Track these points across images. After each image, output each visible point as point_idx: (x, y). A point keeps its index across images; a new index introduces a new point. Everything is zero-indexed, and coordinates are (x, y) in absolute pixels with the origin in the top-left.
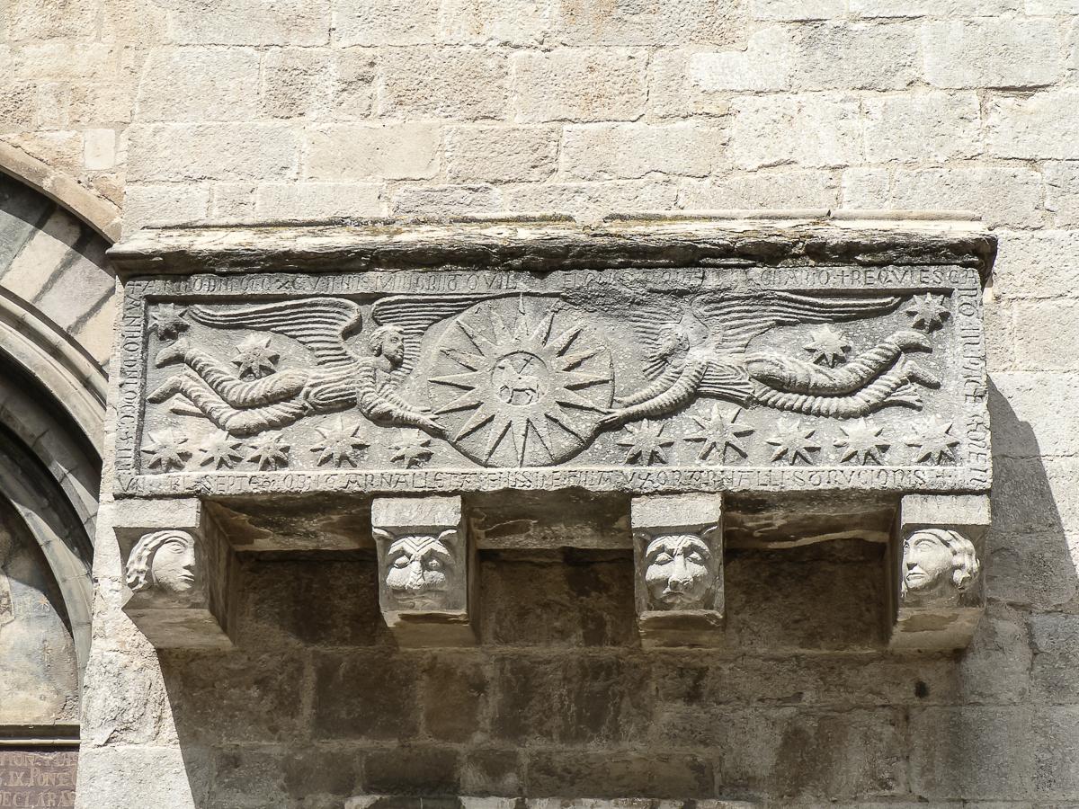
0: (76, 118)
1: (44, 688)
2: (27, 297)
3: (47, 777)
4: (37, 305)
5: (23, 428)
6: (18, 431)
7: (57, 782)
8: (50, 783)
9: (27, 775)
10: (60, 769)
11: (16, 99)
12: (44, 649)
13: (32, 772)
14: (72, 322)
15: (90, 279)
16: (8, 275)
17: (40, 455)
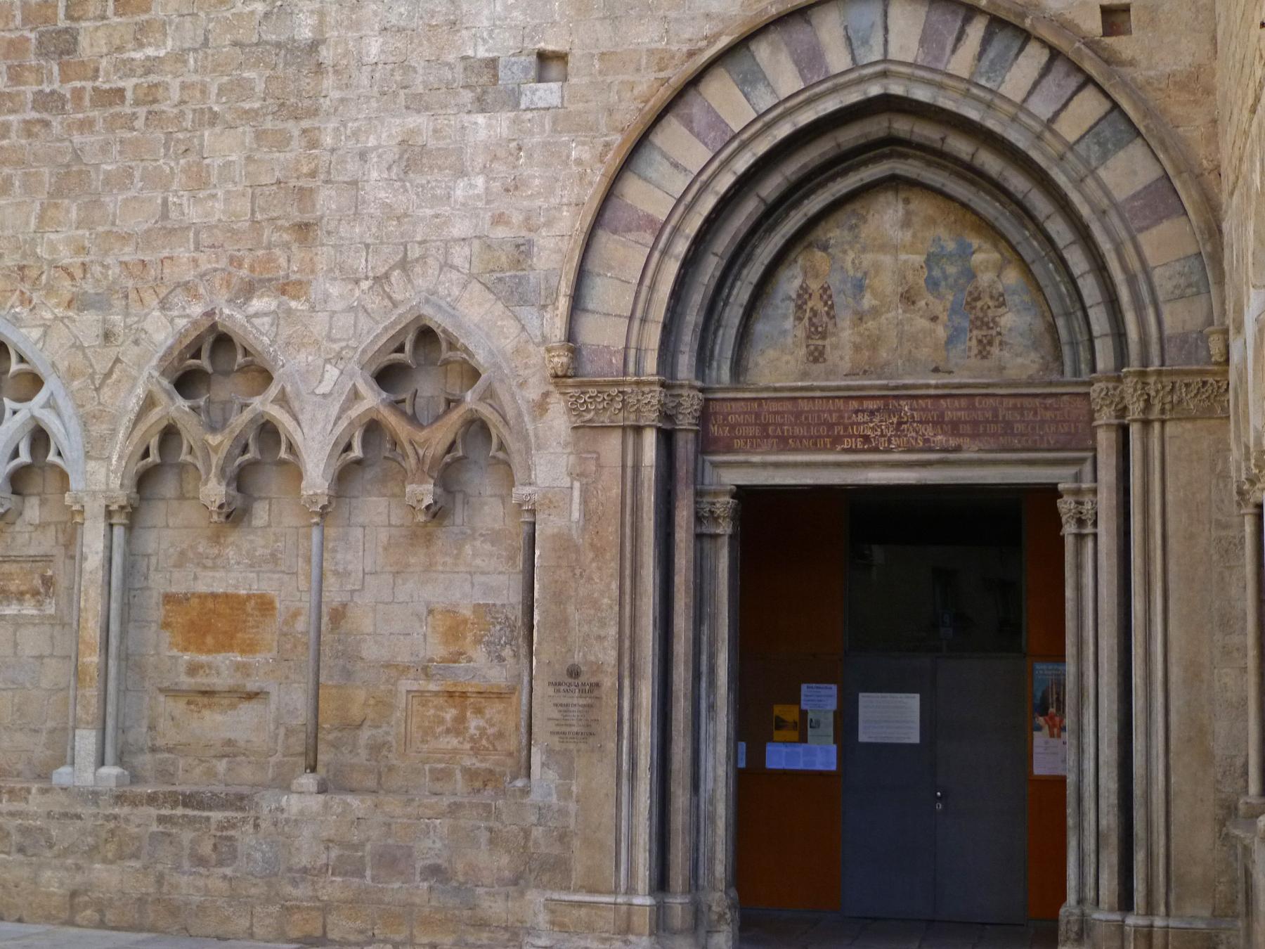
1: (1033, 355)
2: (1018, 99)
3: (1048, 415)
6: (1012, 189)
9: (1036, 414)
14: (1050, 115)
15: (1059, 85)
17: (1028, 205)
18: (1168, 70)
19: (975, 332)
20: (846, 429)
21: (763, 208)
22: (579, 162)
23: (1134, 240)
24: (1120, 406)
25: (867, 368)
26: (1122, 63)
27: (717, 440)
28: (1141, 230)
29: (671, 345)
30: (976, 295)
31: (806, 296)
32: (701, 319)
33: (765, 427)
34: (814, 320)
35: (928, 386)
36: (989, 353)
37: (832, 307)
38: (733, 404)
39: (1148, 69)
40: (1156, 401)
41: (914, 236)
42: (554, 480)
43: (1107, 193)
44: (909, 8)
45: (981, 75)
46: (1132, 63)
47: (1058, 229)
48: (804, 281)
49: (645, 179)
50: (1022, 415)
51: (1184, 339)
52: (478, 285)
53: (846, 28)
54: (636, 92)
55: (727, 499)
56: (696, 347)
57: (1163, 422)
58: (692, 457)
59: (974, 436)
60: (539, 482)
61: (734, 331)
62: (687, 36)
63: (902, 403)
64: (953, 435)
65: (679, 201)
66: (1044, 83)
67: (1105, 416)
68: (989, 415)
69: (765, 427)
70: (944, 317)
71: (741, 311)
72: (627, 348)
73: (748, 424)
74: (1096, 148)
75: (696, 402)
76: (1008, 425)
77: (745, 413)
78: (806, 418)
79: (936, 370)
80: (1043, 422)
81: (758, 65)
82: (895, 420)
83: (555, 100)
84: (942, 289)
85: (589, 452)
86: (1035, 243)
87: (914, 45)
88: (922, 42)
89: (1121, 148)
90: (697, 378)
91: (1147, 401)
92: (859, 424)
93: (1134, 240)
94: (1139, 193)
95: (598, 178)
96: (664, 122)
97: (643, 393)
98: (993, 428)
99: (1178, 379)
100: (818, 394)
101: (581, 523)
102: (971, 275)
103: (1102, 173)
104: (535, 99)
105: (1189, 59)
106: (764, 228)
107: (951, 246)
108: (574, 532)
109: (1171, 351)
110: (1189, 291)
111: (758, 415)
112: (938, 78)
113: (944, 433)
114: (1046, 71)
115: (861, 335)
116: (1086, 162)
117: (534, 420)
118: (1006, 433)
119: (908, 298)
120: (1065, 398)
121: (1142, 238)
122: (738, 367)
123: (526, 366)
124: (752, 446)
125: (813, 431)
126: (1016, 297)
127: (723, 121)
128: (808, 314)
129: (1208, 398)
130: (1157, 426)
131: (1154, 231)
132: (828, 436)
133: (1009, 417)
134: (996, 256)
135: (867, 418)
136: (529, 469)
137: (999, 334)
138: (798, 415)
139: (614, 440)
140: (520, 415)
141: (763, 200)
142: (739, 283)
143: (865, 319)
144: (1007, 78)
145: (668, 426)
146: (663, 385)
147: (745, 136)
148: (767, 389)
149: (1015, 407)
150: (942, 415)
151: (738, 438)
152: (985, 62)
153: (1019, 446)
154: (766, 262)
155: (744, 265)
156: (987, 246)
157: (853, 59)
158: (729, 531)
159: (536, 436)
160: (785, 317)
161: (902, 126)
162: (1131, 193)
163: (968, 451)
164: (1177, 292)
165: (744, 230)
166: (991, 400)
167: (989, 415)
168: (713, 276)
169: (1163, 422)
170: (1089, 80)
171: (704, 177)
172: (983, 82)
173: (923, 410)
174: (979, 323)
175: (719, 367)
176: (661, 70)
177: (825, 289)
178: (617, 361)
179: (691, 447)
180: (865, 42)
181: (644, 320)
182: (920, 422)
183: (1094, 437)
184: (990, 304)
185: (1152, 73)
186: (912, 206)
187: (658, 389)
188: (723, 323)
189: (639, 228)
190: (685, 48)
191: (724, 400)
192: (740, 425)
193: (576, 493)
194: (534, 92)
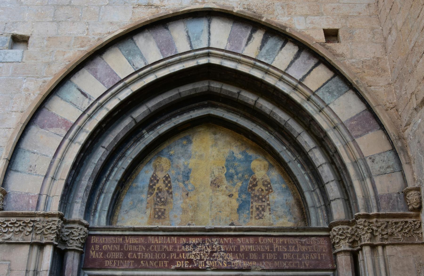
0: (290, 13)
1: (289, 217)
2: (283, 69)
3: (304, 248)
4: (286, 72)
5: (280, 118)
7: (308, 250)
8: (305, 250)
9: (296, 247)
10: (308, 245)
11: (268, 7)
12: (287, 203)
13: (298, 246)
14: (301, 77)
15: (305, 63)
16: (274, 62)
18: (362, 59)
19: (255, 204)
20: (178, 255)
21: (134, 124)
22: (27, 90)
23: (354, 141)
24: (350, 240)
25: (190, 222)
26: (338, 55)
27: (95, 260)
28: (357, 137)
29: (71, 199)
30: (255, 183)
31: (155, 181)
32: (91, 184)
33: (125, 253)
34: (160, 194)
35: (230, 230)
36: (263, 216)
37: (170, 188)
38: (107, 238)
39: (351, 59)
40: (377, 234)
41: (219, 151)
43: (337, 117)
44: (222, 24)
45: (262, 57)
46: (342, 55)
47: (306, 141)
48: (154, 173)
49: (66, 101)
50: (288, 248)
51: (389, 197)
53: (187, 32)
54: (66, 56)
56: (86, 200)
57: (384, 246)
58: (76, 268)
59: (258, 261)
61: (110, 195)
62: (99, 32)
63: (214, 240)
64: (245, 260)
65: (84, 113)
66: (296, 61)
67: (344, 246)
68: (268, 248)
69: (125, 253)
70: (236, 195)
71: (116, 183)
72: (40, 195)
73: (115, 251)
74: (328, 94)
75: (82, 233)
76: (279, 254)
77: (114, 244)
78: (153, 248)
79: (232, 224)
80: (301, 252)
81: (137, 47)
82: (209, 250)
83: (18, 58)
84: (235, 181)
85: (4, 260)
86: (289, 153)
87: (225, 41)
88: (229, 40)
89: (341, 95)
91: (372, 233)
92: (186, 252)
93: (354, 141)
94: (354, 117)
95: (35, 98)
96: (80, 72)
97: (48, 222)
98: (270, 256)
99: (390, 220)
100: (161, 233)
102: (251, 172)
103: (331, 106)
104: (6, 57)
105: (372, 55)
106: (133, 139)
107: (240, 156)
109: (383, 204)
110: (389, 170)
111: (122, 246)
112: (238, 57)
113: (241, 259)
114: (297, 56)
115: (186, 203)
116: (323, 102)
118: (278, 260)
119: (215, 184)
120: (313, 238)
121: (357, 140)
122: (112, 215)
124: (116, 265)
125: (157, 256)
126: (277, 185)
127: (115, 73)
128: (156, 191)
129: (409, 231)
130: (380, 249)
131: (365, 137)
132: (166, 260)
133: (280, 249)
134: (266, 163)
135: (191, 249)
137: (269, 205)
138: (147, 246)
141: (134, 120)
142: (116, 169)
143: (189, 195)
144: (277, 58)
145: (63, 248)
146: (61, 217)
147: (127, 81)
148: (129, 229)
149: (283, 244)
150: (238, 247)
151: (108, 259)
152: (264, 50)
153: (287, 267)
154: (133, 157)
155: (120, 159)
156: (260, 158)
157: (191, 46)
160: (142, 192)
161: (216, 86)
162: (350, 117)
163: (254, 270)
164: (382, 170)
165: (122, 136)
166: (269, 240)
167: (268, 248)
168: (100, 159)
169: (384, 246)
170: (321, 60)
171: (101, 101)
172: (263, 60)
173: (226, 244)
174: (256, 198)
175: (100, 216)
176: (82, 47)
177: (167, 178)
178: (33, 202)
179: (76, 262)
180: (198, 38)
181: (53, 179)
182: (225, 252)
183: (335, 262)
184: (263, 188)
185: (354, 60)
186: (218, 136)
187: (57, 219)
188: (105, 191)
189: (58, 126)
190: (96, 38)
192: (110, 251)
194: (6, 54)
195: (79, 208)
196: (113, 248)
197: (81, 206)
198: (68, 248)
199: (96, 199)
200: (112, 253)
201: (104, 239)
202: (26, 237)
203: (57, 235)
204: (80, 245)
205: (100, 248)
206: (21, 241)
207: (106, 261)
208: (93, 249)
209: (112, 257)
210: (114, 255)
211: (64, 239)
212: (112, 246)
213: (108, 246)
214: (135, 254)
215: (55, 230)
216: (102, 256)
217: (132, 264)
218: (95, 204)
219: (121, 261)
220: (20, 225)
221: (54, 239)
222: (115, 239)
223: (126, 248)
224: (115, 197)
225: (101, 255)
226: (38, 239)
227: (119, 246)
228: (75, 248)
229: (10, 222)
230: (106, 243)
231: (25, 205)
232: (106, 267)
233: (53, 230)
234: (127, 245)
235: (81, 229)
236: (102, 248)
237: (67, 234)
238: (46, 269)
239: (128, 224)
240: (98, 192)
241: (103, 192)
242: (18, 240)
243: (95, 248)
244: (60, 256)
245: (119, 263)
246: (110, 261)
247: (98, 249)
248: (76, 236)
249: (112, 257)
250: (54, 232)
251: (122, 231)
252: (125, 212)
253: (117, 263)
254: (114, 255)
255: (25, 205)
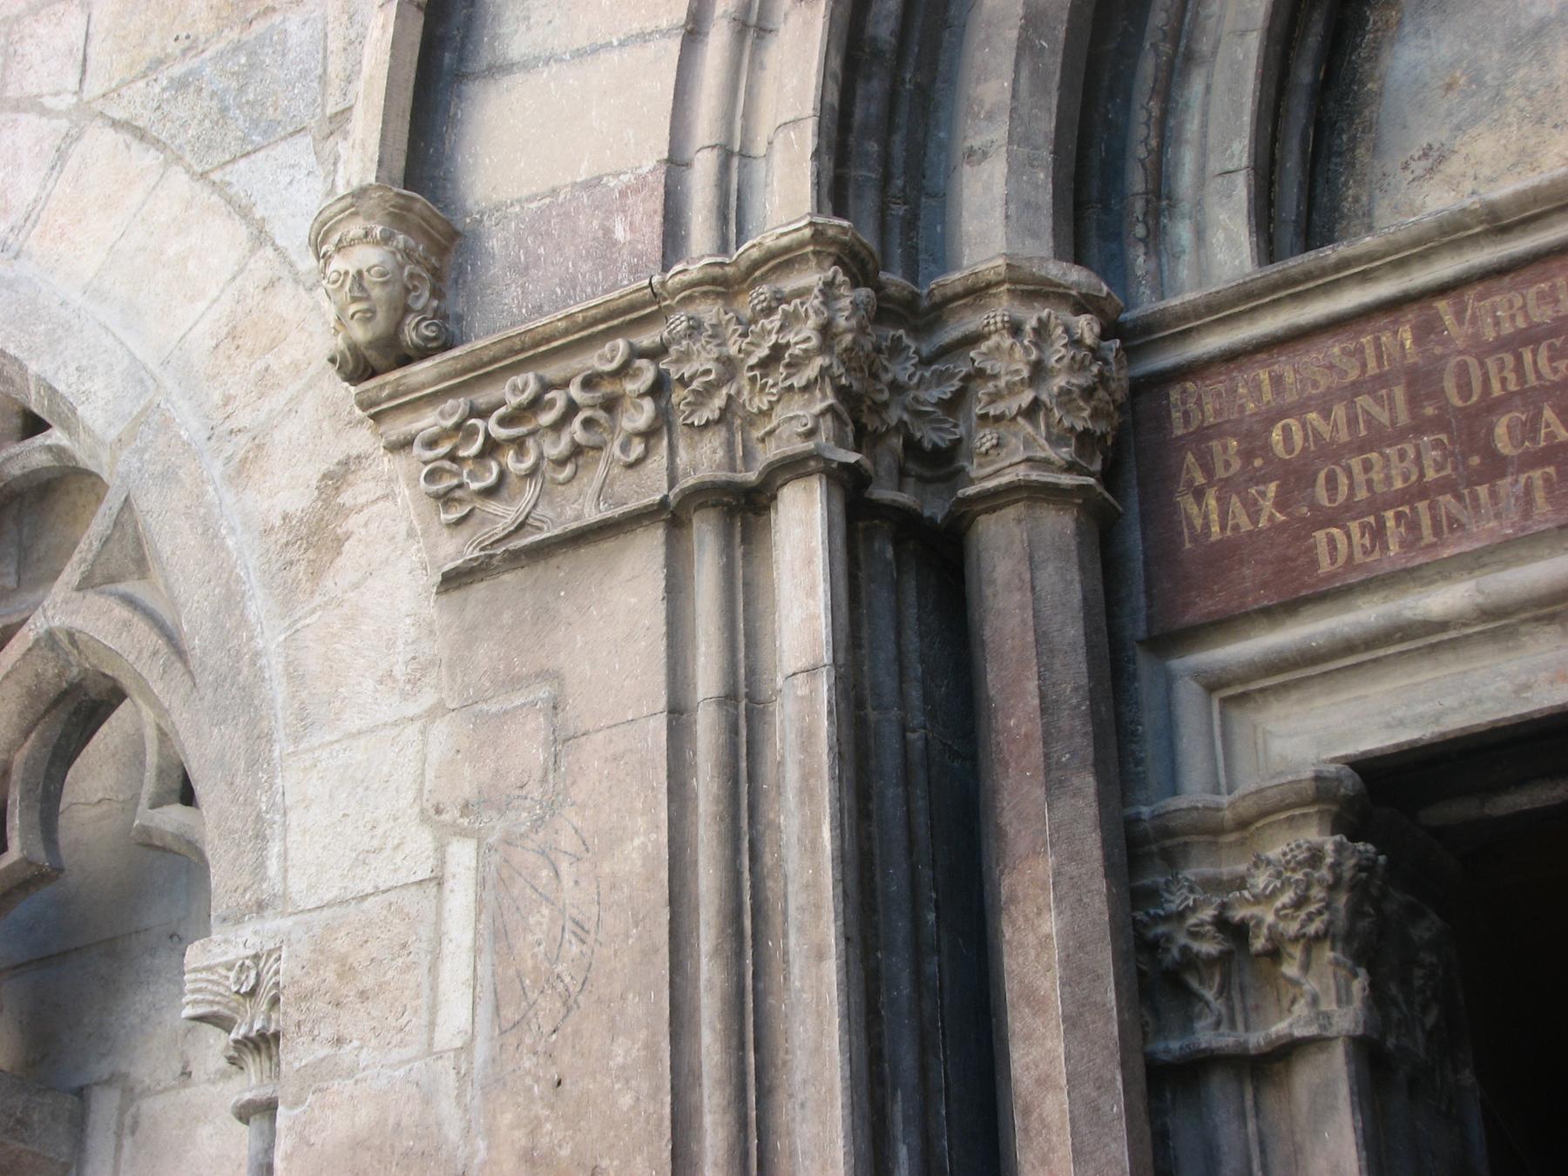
27: (1225, 555)
33: (1467, 430)
38: (1284, 365)
42: (363, 859)
52: (109, 135)
55: (1315, 835)
56: (1046, 124)
60: (297, 885)
69: (1467, 430)
73: (1377, 439)
75: (1058, 351)
77: (1356, 388)
85: (514, 682)
90: (1075, 248)
101: (481, 1051)
108: (447, 1107)
117: (287, 598)
123: (265, 382)
136: (260, 837)
139: (633, 579)
140: (231, 600)
145: (936, 509)
158: (1347, 1019)
159: (295, 676)
178: (638, 228)
191: (1232, 357)
192: (1331, 452)
193: (460, 899)
195: (999, 190)
196: (1352, 421)
197: (1014, 171)
198: (971, 490)
199: (1142, 116)
200: (1356, 463)
201: (1264, 376)
202: (632, 476)
203: (841, 392)
204: (1066, 453)
205: (1247, 455)
206: (592, 516)
207: (1320, 535)
208: (1200, 479)
209: (1362, 494)
210: (1377, 476)
211: (930, 437)
212: (1339, 412)
213: (1313, 416)
214: (1548, 414)
215: (808, 355)
216: (1281, 503)
217: (1539, 496)
218: (1141, 152)
219: (1446, 499)
220: (572, 408)
221: (827, 424)
222: (1361, 350)
223: (1465, 389)
224: (1304, 74)
225: (1267, 505)
226: (704, 460)
227: (1399, 393)
228: (1021, 473)
229: (502, 410)
230: (1291, 398)
231: (586, 267)
232: (1332, 576)
233: (795, 365)
234: (1463, 369)
235: (1042, 330)
236: (1267, 448)
237: (946, 391)
238: (803, 663)
239: (1437, 200)
240: (1148, 67)
241: (1190, 58)
242: (577, 518)
243: (1208, 470)
244: (909, 558)
245: (1426, 522)
246: (1354, 527)
247: (1237, 464)
248: (1012, 389)
249: (1362, 494)
250: (811, 371)
251: (1401, 265)
252: (1419, 167)
253: (1414, 526)
254: (1377, 476)
255: (586, 267)
